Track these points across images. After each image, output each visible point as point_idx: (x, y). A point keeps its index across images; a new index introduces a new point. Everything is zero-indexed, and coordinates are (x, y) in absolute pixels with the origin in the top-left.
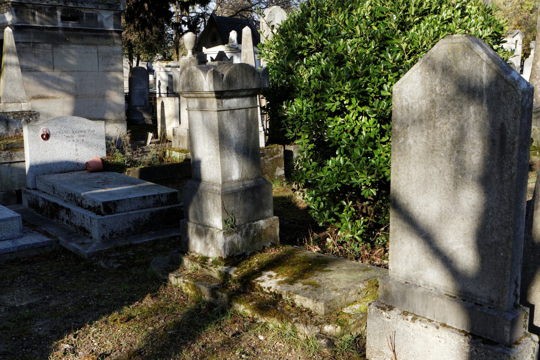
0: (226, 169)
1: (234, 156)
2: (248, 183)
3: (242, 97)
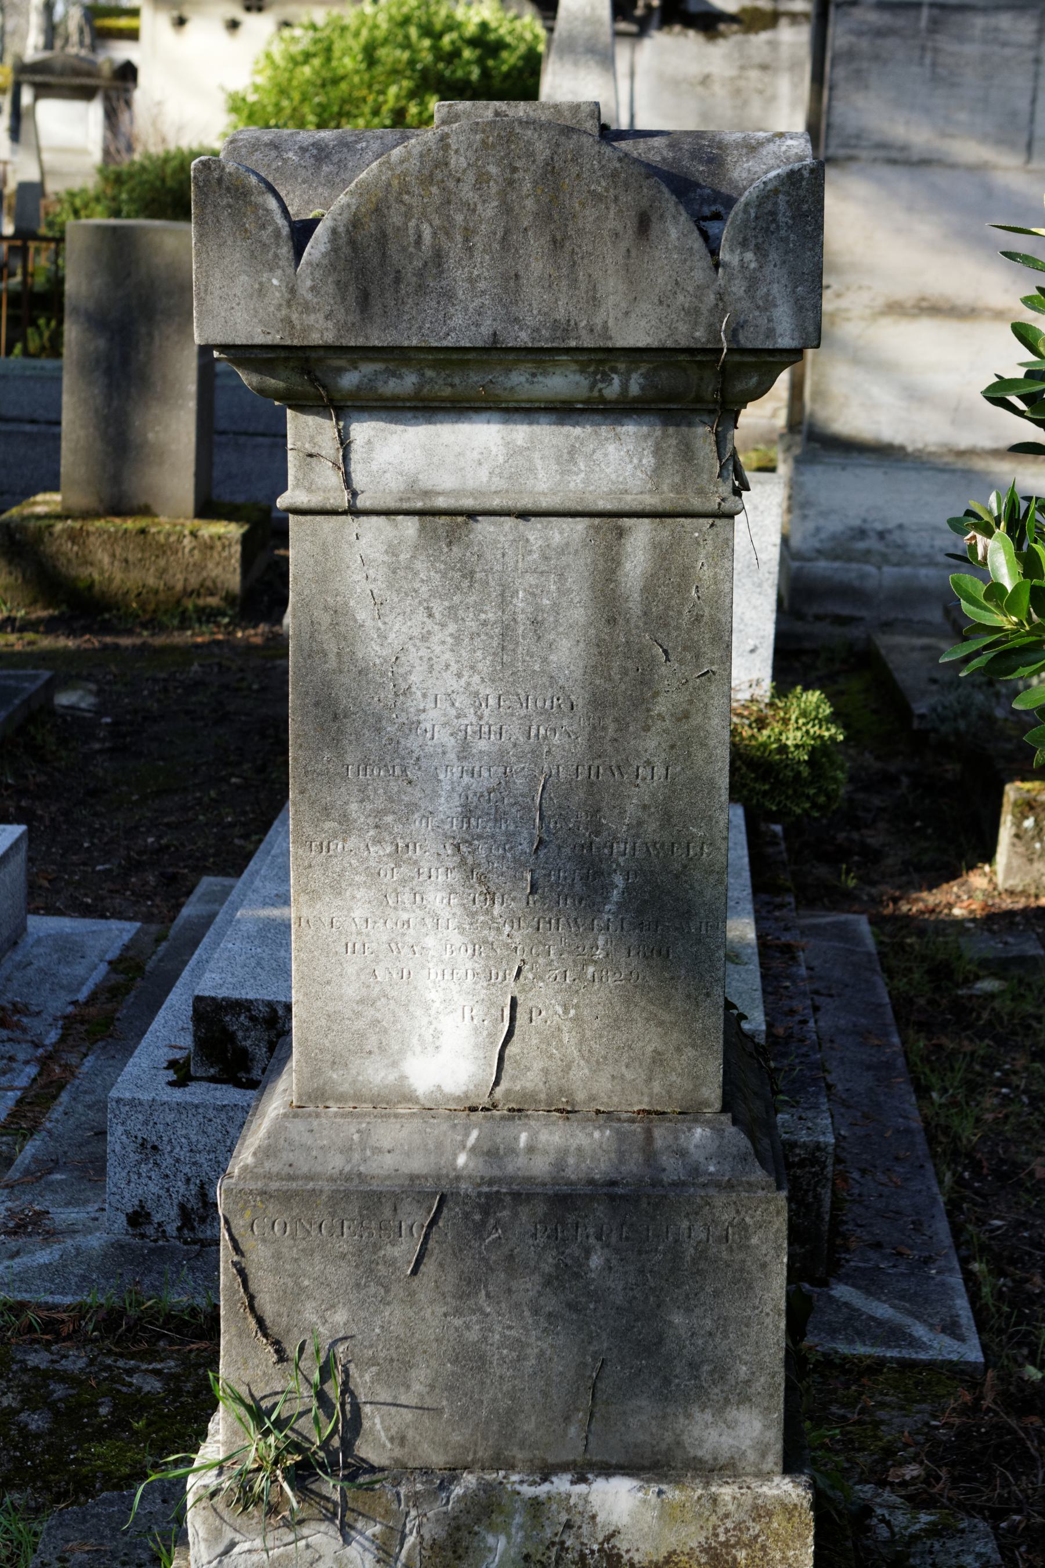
0: (351, 991)
1: (436, 899)
2: (544, 1146)
3: (563, 411)
